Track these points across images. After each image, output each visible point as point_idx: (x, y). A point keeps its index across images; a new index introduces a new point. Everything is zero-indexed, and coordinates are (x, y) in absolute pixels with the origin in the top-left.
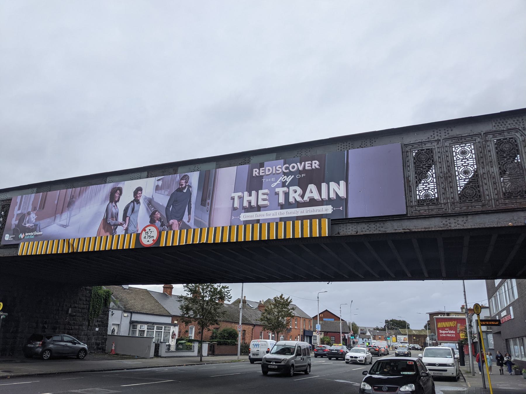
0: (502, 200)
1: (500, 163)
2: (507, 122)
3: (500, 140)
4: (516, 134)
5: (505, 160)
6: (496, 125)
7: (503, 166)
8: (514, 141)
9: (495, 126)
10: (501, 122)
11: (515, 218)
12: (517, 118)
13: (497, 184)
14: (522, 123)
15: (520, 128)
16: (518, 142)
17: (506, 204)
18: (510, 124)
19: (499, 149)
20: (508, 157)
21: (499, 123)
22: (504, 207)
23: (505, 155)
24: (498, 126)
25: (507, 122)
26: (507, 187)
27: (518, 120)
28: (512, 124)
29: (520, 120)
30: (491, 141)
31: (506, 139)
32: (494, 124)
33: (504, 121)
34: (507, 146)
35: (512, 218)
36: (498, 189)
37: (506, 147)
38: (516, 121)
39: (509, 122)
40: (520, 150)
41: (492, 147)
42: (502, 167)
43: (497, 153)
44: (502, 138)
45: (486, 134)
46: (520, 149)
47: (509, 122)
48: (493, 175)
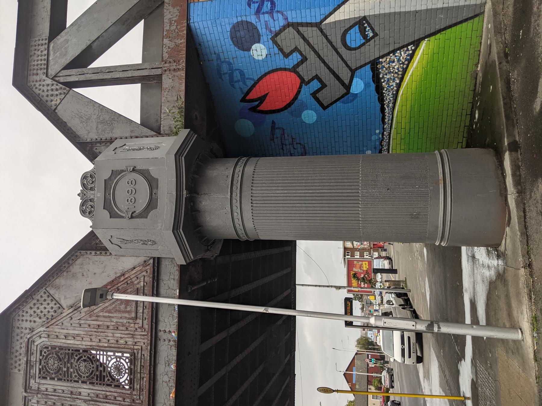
0: (135, 393)
1: (76, 379)
2: (17, 351)
3: (40, 370)
4: (36, 344)
5: (72, 370)
6: (18, 368)
7: (81, 376)
8: (45, 350)
9: (19, 370)
10: (14, 359)
11: (166, 379)
12: (14, 334)
13: (108, 393)
14: (23, 330)
15: (28, 336)
16: (49, 343)
17: (141, 390)
18: (21, 348)
19: (53, 376)
20: (69, 365)
21: (16, 362)
22: (145, 392)
23: (65, 369)
24: (20, 365)
25: (17, 351)
26: (122, 361)
27: (18, 335)
28: (21, 343)
29: (18, 331)
30: (39, 384)
31: (40, 360)
32: (16, 371)
33: (15, 354)
34: (51, 362)
35: (165, 384)
36: (116, 394)
37: (53, 363)
38: (19, 338)
39: (18, 348)
40: (62, 345)
41: (48, 385)
42: (83, 379)
43: (60, 379)
44: (38, 365)
45: (27, 388)
46: (59, 344)
47: (18, 348)
48: (92, 395)
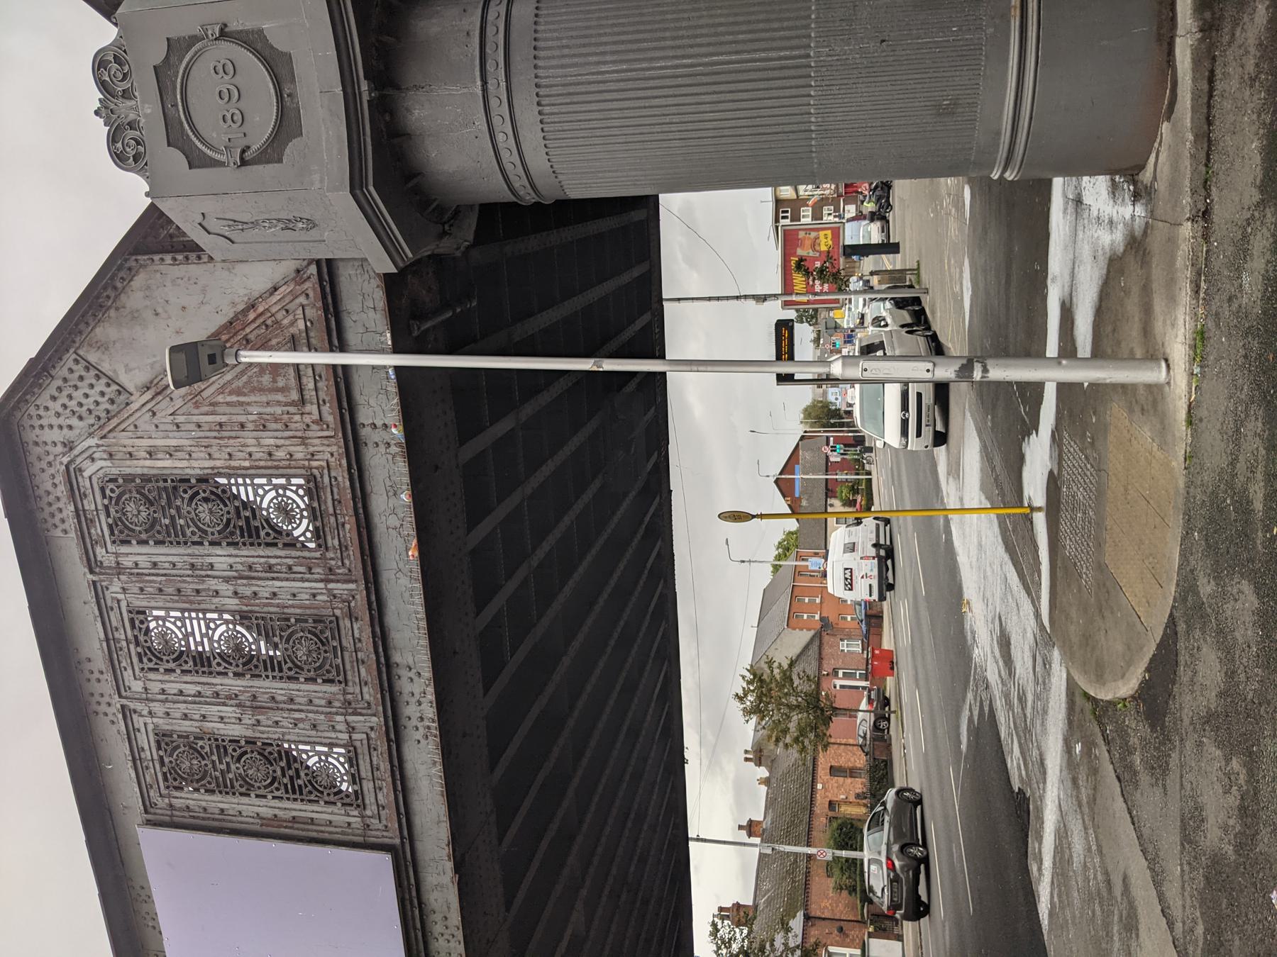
0: (330, 554)
1: (196, 539)
2: (48, 493)
3: (110, 527)
4: (86, 474)
5: (182, 522)
7: (205, 532)
8: (111, 486)
9: (65, 532)
10: (47, 510)
12: (32, 459)
13: (273, 561)
15: (65, 460)
16: (115, 471)
17: (343, 547)
18: (55, 485)
19: (144, 536)
20: (173, 512)
21: (53, 515)
23: (167, 521)
24: (63, 521)
26: (289, 493)
29: (38, 450)
30: (117, 555)
31: (106, 508)
32: (58, 533)
33: (45, 500)
34: (131, 508)
37: (136, 512)
38: (44, 465)
40: (146, 471)
41: (137, 555)
43: (158, 543)
44: (103, 517)
45: (92, 565)
46: (139, 471)
48: (240, 567)
